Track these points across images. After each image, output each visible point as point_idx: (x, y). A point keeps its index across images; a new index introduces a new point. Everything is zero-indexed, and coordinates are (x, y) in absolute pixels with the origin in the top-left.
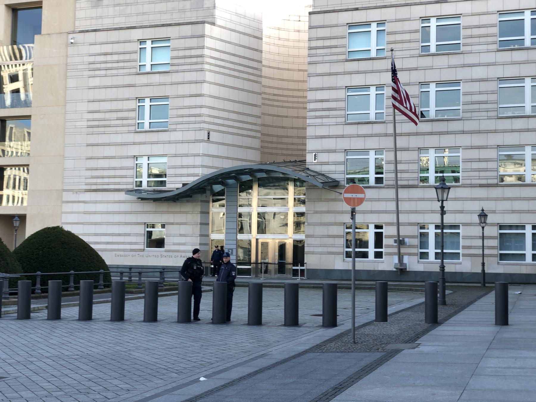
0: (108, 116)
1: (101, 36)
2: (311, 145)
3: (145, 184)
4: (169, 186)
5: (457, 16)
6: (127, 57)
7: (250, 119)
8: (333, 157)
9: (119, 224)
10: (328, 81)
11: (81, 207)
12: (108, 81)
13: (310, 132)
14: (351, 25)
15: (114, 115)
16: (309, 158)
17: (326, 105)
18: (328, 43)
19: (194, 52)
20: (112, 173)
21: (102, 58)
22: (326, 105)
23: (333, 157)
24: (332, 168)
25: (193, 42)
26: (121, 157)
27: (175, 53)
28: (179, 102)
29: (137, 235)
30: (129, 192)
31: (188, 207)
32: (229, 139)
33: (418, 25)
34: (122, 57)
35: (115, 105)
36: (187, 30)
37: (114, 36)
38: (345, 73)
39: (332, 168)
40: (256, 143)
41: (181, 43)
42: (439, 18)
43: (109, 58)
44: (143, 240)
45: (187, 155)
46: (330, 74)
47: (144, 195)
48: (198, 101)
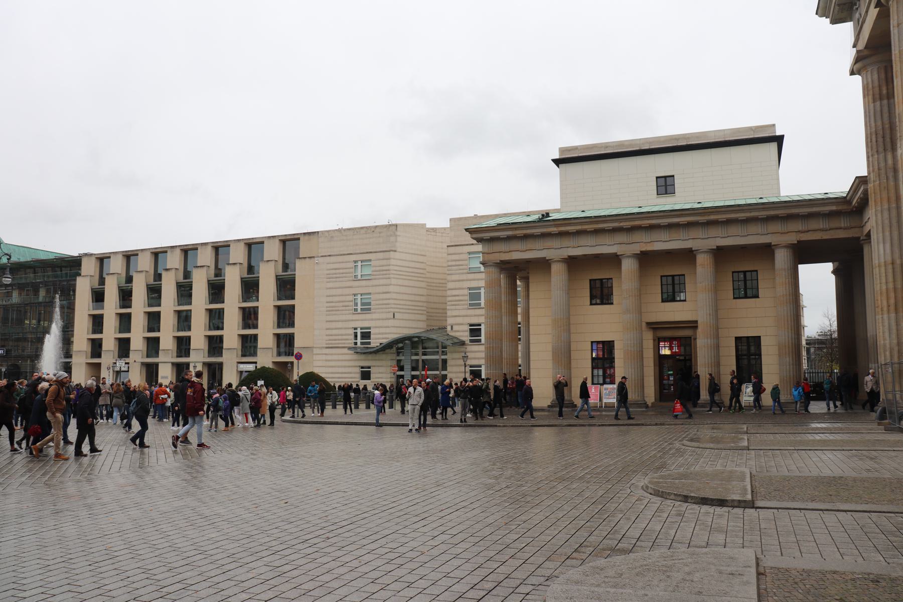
0: (337, 304)
1: (332, 259)
2: (450, 321)
3: (359, 344)
4: (372, 345)
7: (419, 304)
9: (345, 367)
10: (458, 285)
11: (324, 357)
13: (449, 313)
14: (469, 253)
15: (341, 304)
16: (449, 328)
17: (457, 298)
18: (457, 263)
19: (384, 268)
20: (340, 337)
21: (334, 271)
22: (457, 298)
24: (461, 334)
25: (384, 262)
27: (374, 269)
28: (377, 296)
29: (355, 373)
30: (349, 348)
31: (383, 356)
32: (406, 316)
36: (381, 255)
38: (467, 280)
39: (461, 334)
40: (424, 318)
41: (377, 263)
43: (337, 271)
44: (359, 376)
45: (381, 327)
47: (359, 350)
48: (387, 296)
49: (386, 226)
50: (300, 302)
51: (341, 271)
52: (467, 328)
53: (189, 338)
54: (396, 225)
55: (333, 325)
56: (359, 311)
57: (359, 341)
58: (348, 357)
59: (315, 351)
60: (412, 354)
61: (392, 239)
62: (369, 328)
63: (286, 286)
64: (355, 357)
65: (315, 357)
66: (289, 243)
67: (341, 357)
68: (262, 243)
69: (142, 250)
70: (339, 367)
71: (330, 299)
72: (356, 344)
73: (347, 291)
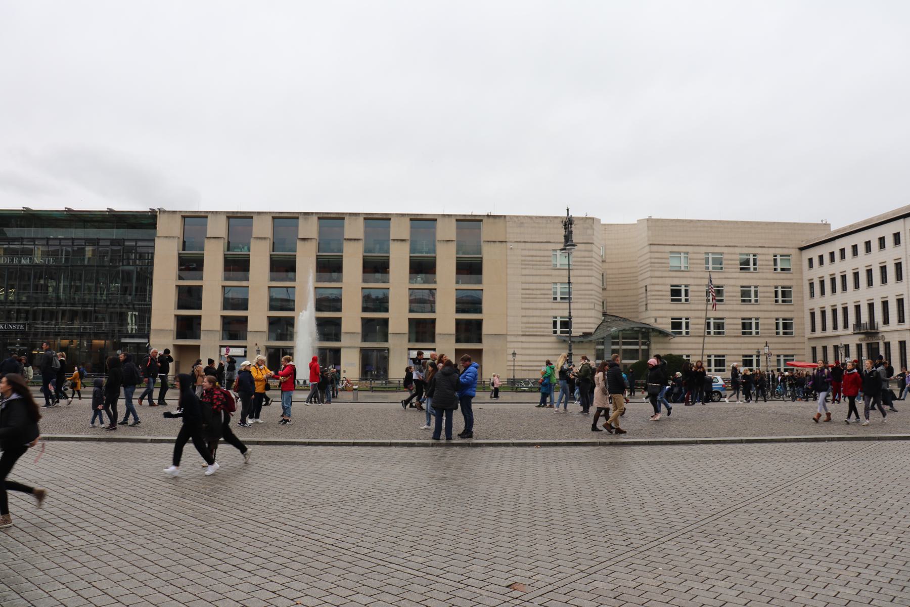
0: (535, 292)
1: (528, 246)
3: (559, 332)
5: (722, 254)
6: (546, 259)
8: (664, 321)
10: (661, 281)
12: (535, 272)
14: (671, 252)
15: (539, 292)
17: (660, 293)
19: (587, 259)
20: (538, 325)
21: (530, 258)
22: (660, 293)
23: (664, 321)
25: (586, 254)
26: (544, 317)
33: (704, 256)
34: (542, 259)
35: (539, 286)
37: (537, 246)
42: (713, 253)
43: (534, 258)
46: (662, 277)
48: (590, 287)
49: (582, 219)
50: (490, 287)
51: (538, 259)
52: (670, 321)
53: (199, 317)
54: (593, 219)
55: (530, 313)
56: (559, 299)
57: (559, 329)
58: (549, 345)
59: (509, 339)
60: (614, 344)
61: (590, 232)
62: (723, 319)
63: (470, 268)
64: (556, 345)
65: (509, 345)
66: (469, 223)
67: (539, 346)
68: (435, 220)
69: (259, 213)
70: (537, 355)
71: (527, 286)
72: (555, 332)
73: (546, 279)
